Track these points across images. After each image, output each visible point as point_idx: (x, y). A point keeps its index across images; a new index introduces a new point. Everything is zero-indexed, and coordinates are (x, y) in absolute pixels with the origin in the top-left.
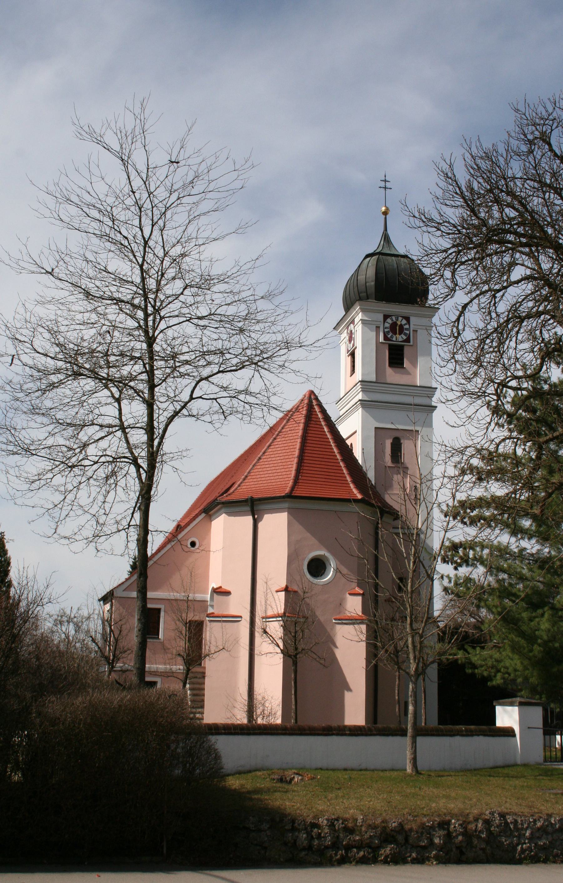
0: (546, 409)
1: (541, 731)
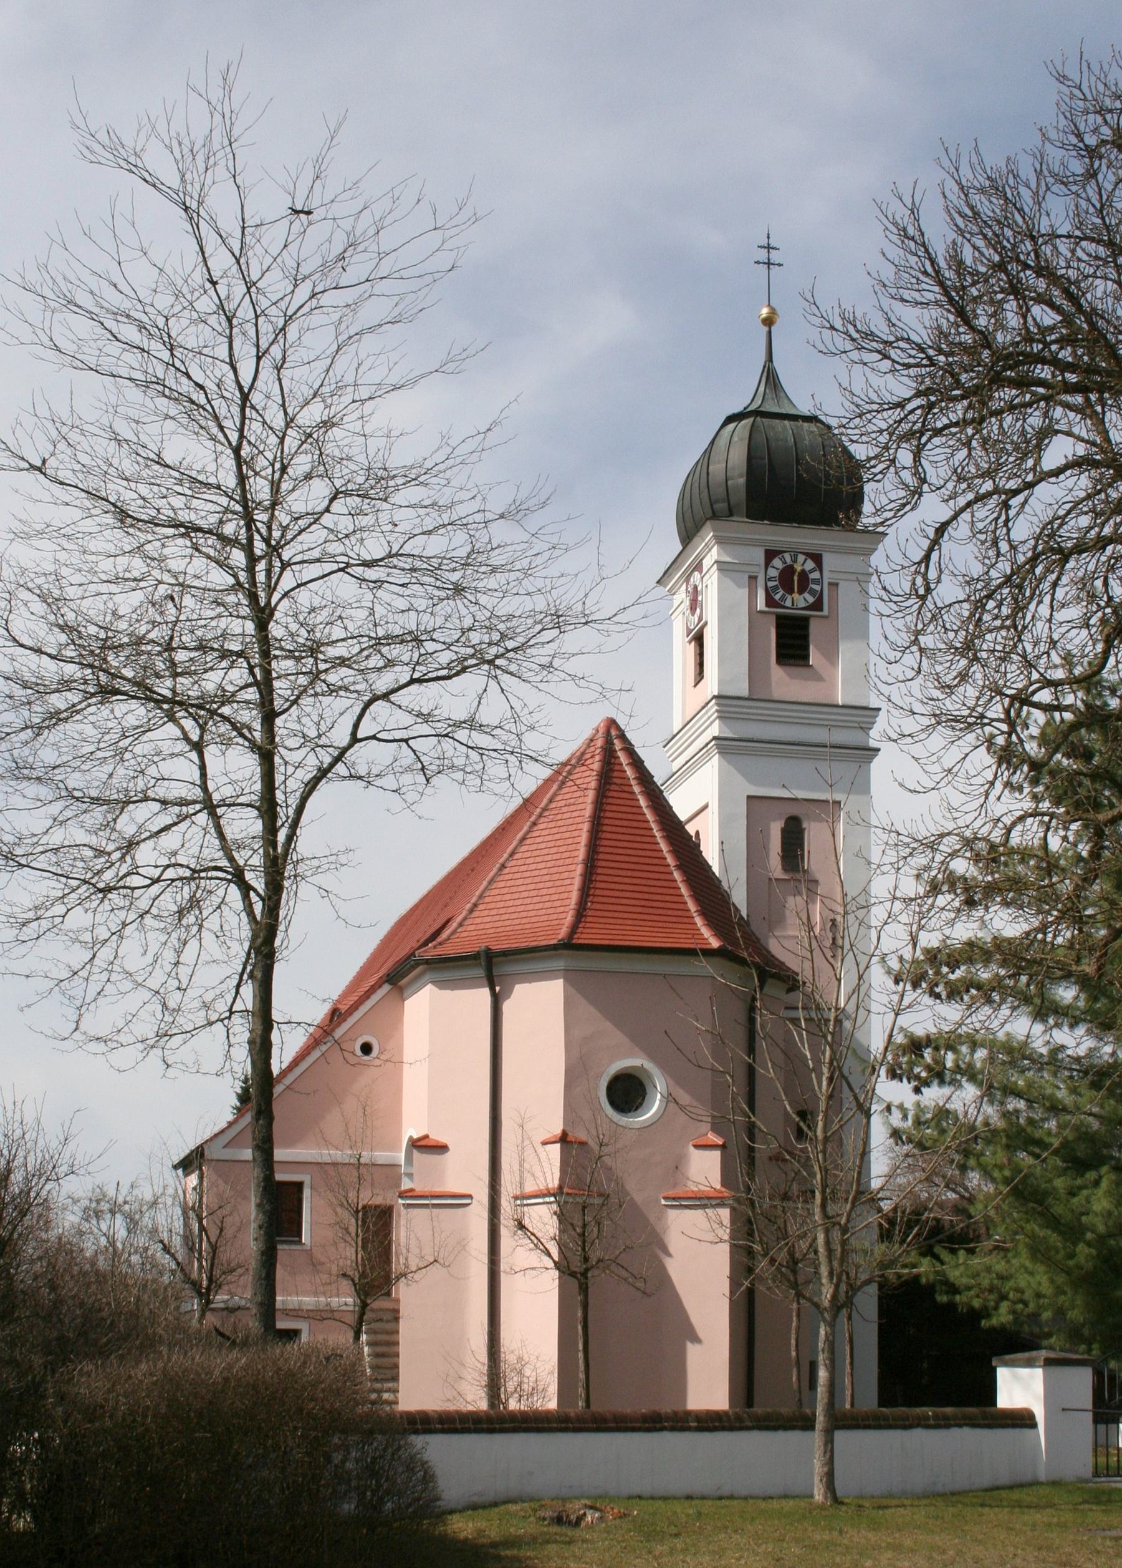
0: (1114, 751)
1: (1089, 1417)
